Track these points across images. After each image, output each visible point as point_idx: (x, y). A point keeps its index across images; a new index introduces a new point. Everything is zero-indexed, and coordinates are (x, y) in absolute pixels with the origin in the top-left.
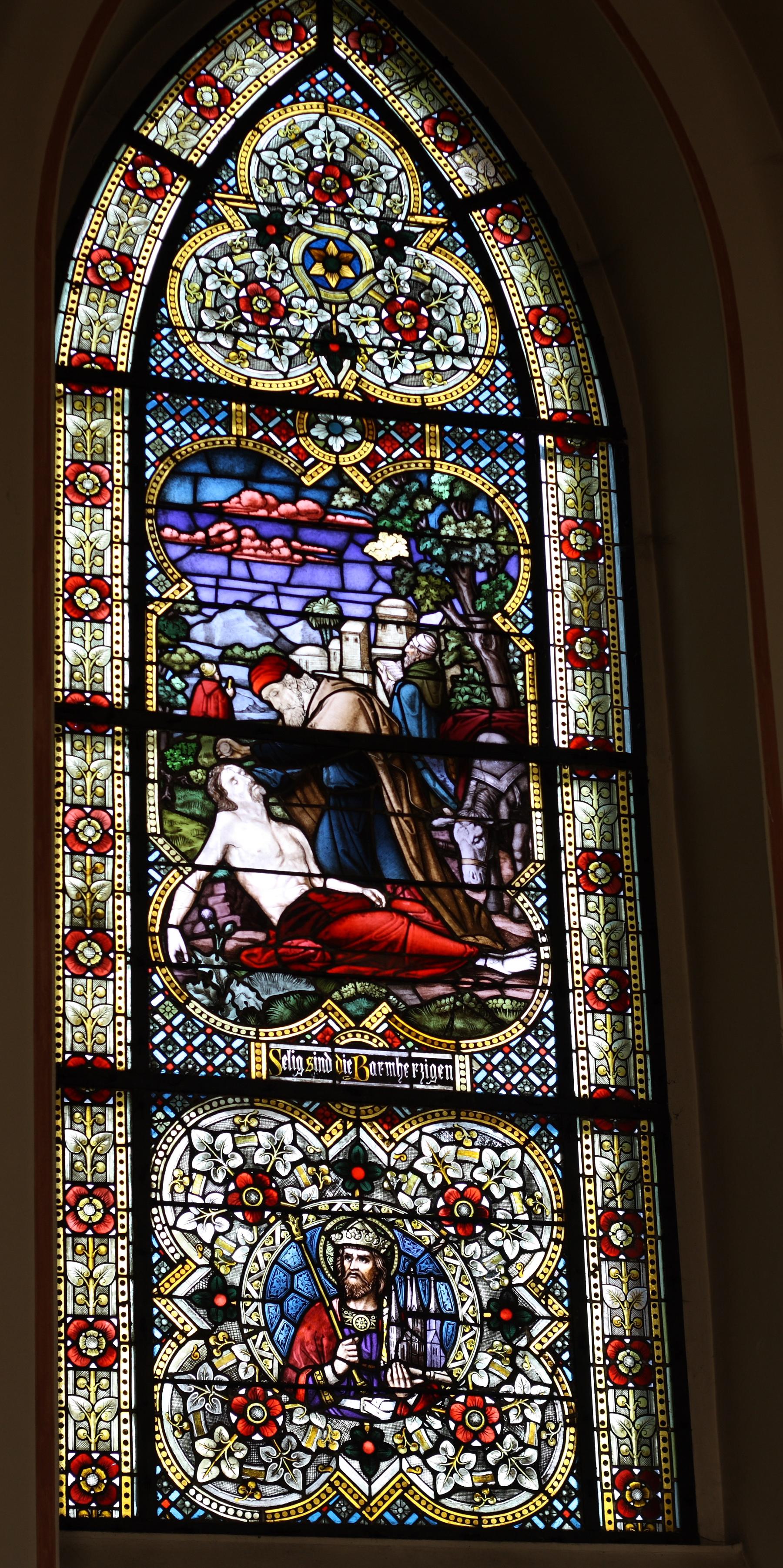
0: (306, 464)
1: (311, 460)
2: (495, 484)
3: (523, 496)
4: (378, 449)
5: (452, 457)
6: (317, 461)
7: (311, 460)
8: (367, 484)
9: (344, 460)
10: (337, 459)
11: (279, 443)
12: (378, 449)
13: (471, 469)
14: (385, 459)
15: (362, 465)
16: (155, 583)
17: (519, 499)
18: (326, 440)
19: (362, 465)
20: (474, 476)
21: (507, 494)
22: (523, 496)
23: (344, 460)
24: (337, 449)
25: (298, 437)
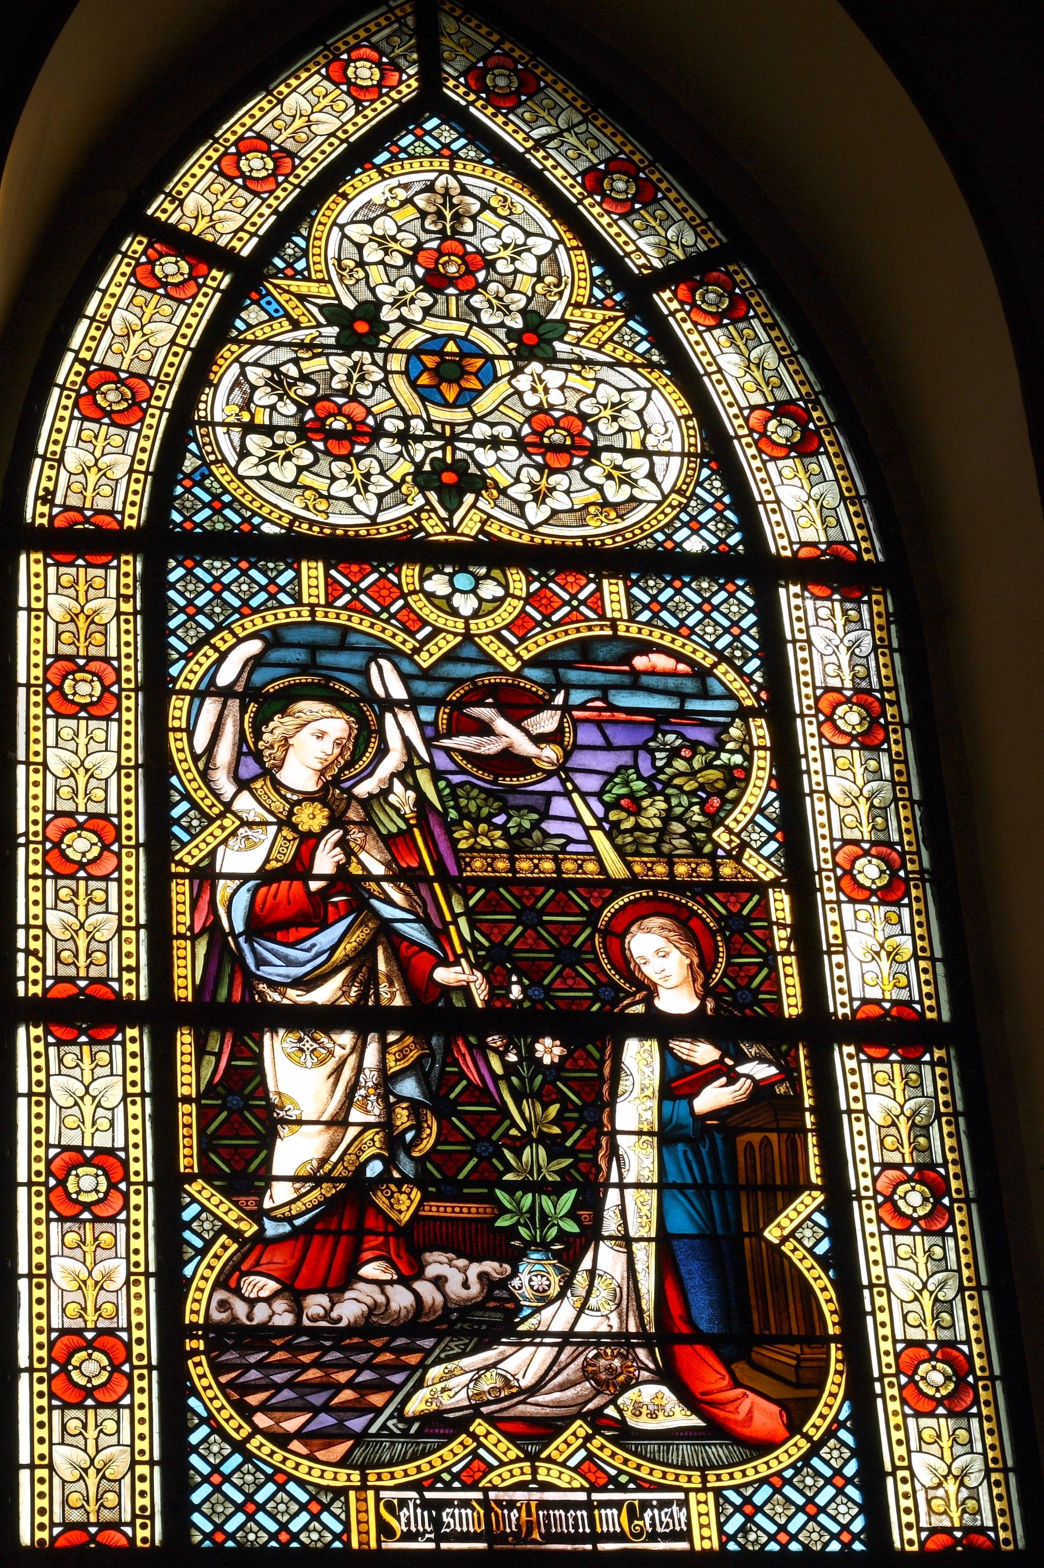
0: (420, 636)
1: (428, 630)
2: (713, 650)
3: (755, 663)
4: (528, 609)
5: (646, 616)
6: (437, 631)
7: (428, 630)
8: (512, 660)
9: (478, 626)
10: (467, 627)
11: (377, 608)
12: (528, 609)
13: (675, 631)
14: (539, 624)
15: (504, 633)
16: (184, 822)
17: (748, 669)
18: (448, 598)
19: (504, 633)
20: (680, 641)
21: (729, 661)
22: (755, 663)
23: (478, 626)
24: (466, 610)
25: (404, 596)
